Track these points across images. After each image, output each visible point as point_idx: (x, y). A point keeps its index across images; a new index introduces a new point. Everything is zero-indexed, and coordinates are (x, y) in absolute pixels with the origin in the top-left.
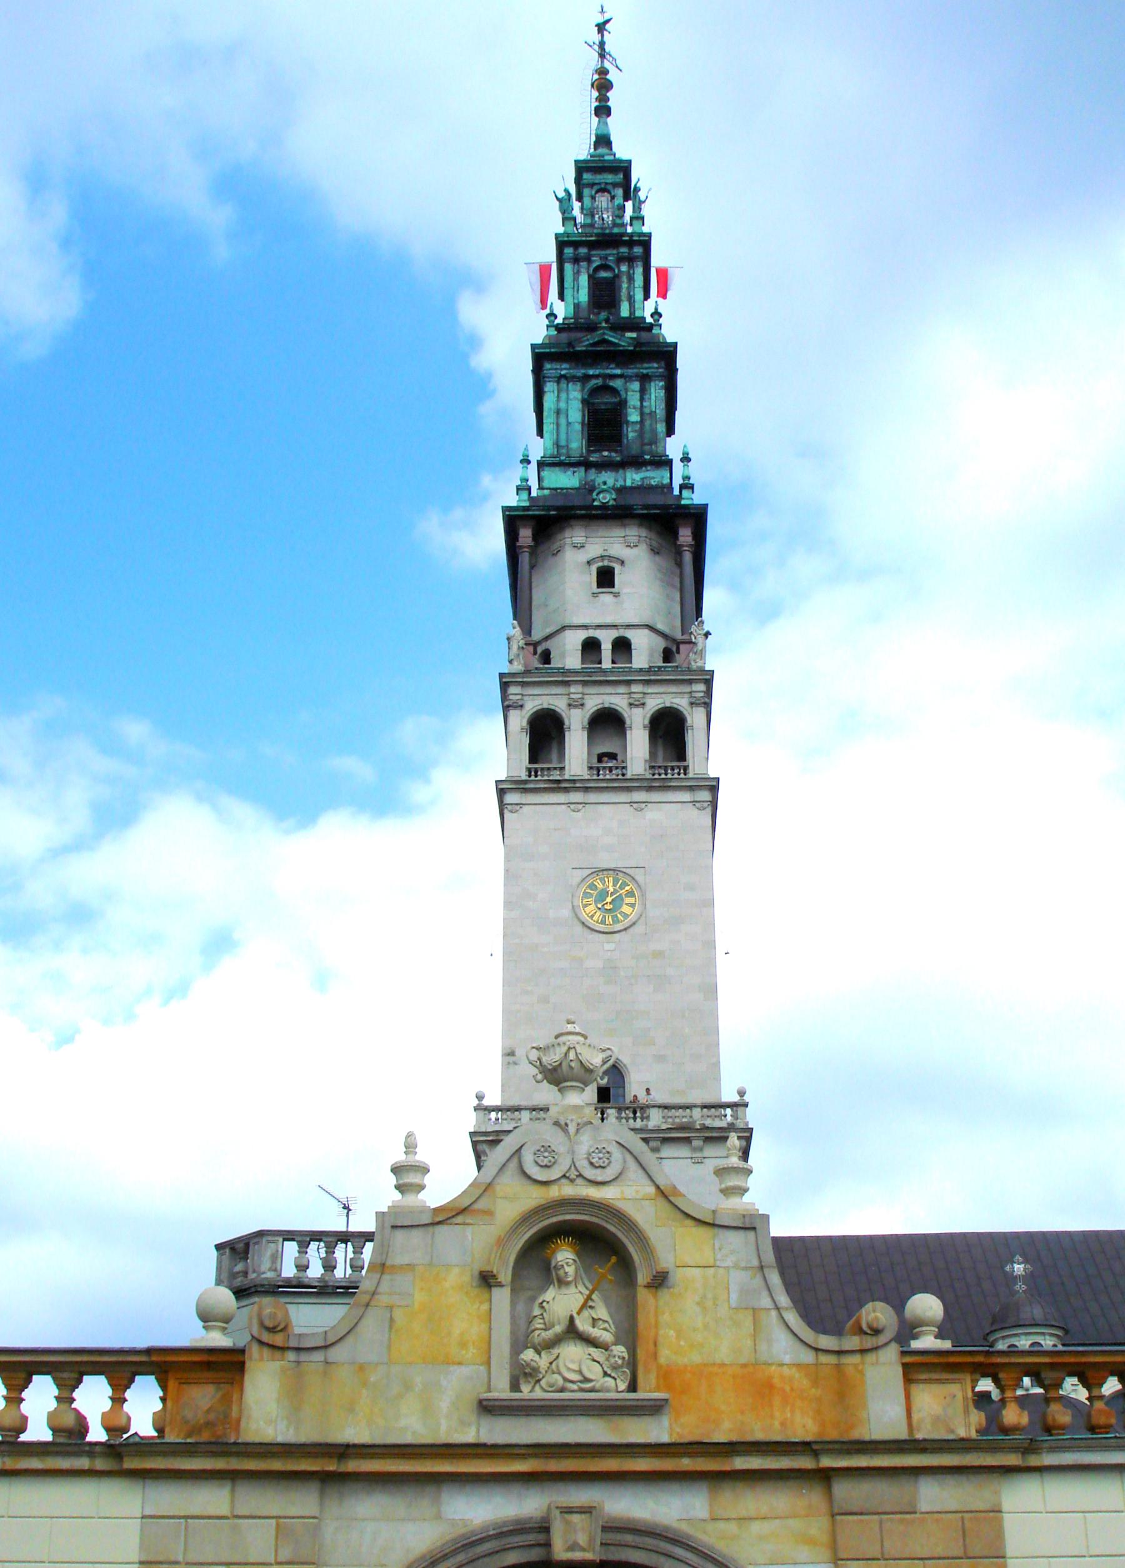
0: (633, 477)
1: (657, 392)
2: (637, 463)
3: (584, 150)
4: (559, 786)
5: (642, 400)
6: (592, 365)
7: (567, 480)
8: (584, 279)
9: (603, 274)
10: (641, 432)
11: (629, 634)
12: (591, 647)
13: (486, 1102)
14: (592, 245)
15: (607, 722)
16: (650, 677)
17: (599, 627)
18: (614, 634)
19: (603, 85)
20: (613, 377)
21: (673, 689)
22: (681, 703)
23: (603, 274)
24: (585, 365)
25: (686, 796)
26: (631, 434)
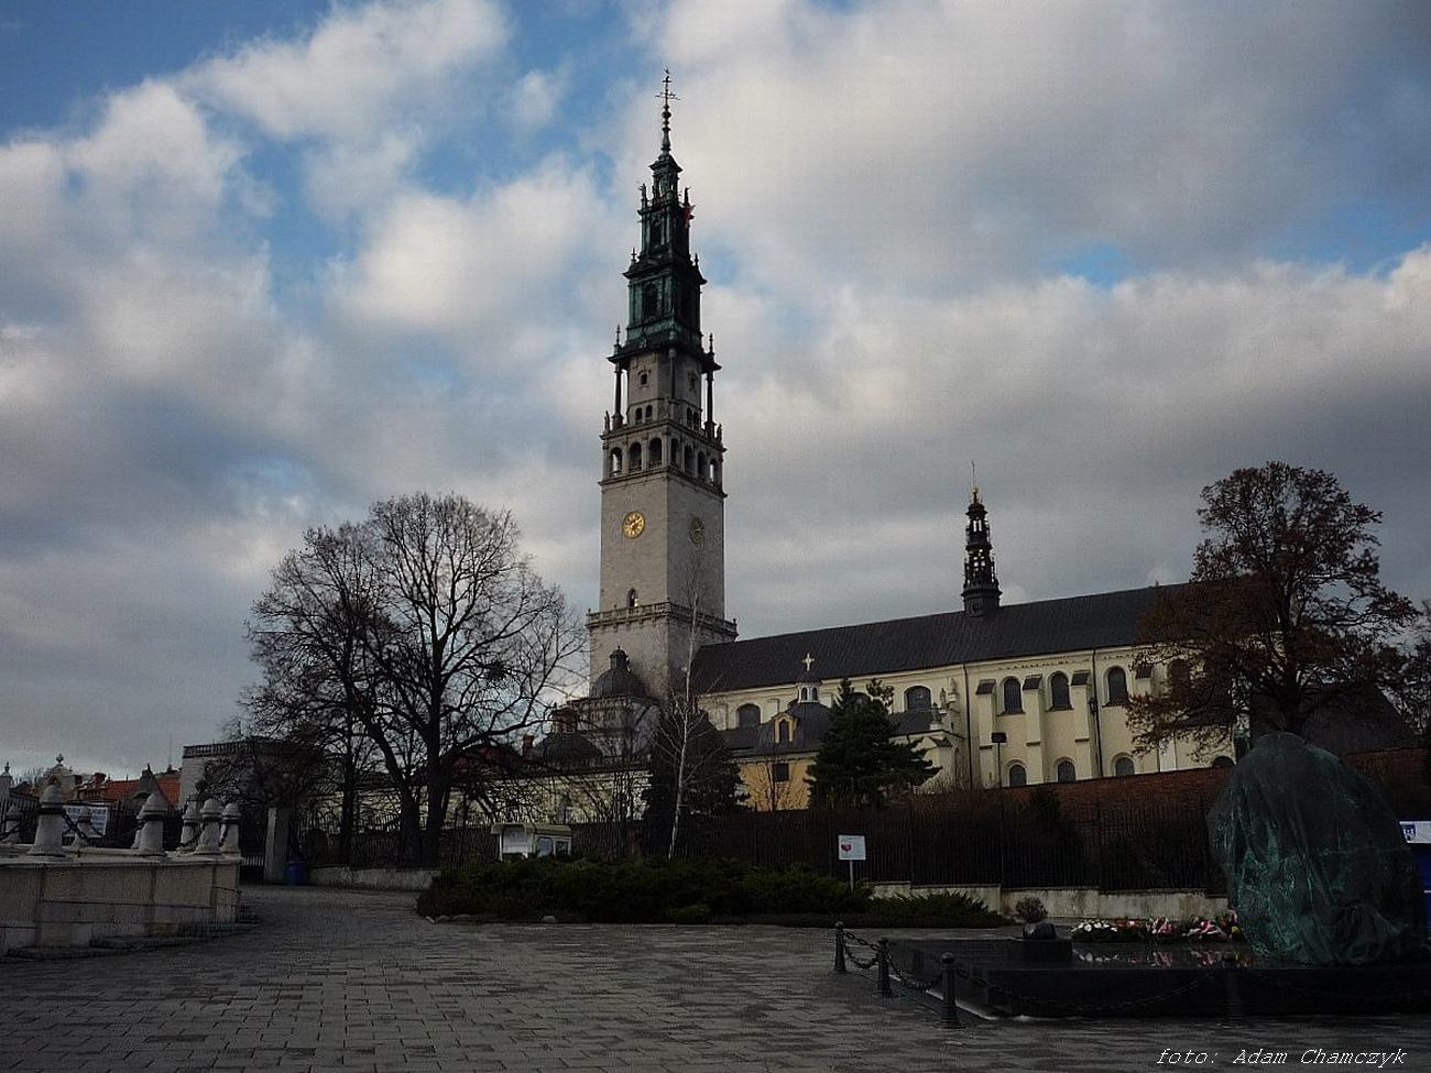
0: (658, 327)
1: (668, 283)
2: (659, 321)
3: (654, 159)
4: (618, 480)
7: (636, 334)
8: (648, 229)
11: (652, 404)
13: (592, 612)
14: (651, 212)
15: (636, 449)
16: (649, 426)
17: (641, 403)
18: (647, 404)
19: (667, 115)
20: (653, 280)
22: (660, 435)
23: (657, 224)
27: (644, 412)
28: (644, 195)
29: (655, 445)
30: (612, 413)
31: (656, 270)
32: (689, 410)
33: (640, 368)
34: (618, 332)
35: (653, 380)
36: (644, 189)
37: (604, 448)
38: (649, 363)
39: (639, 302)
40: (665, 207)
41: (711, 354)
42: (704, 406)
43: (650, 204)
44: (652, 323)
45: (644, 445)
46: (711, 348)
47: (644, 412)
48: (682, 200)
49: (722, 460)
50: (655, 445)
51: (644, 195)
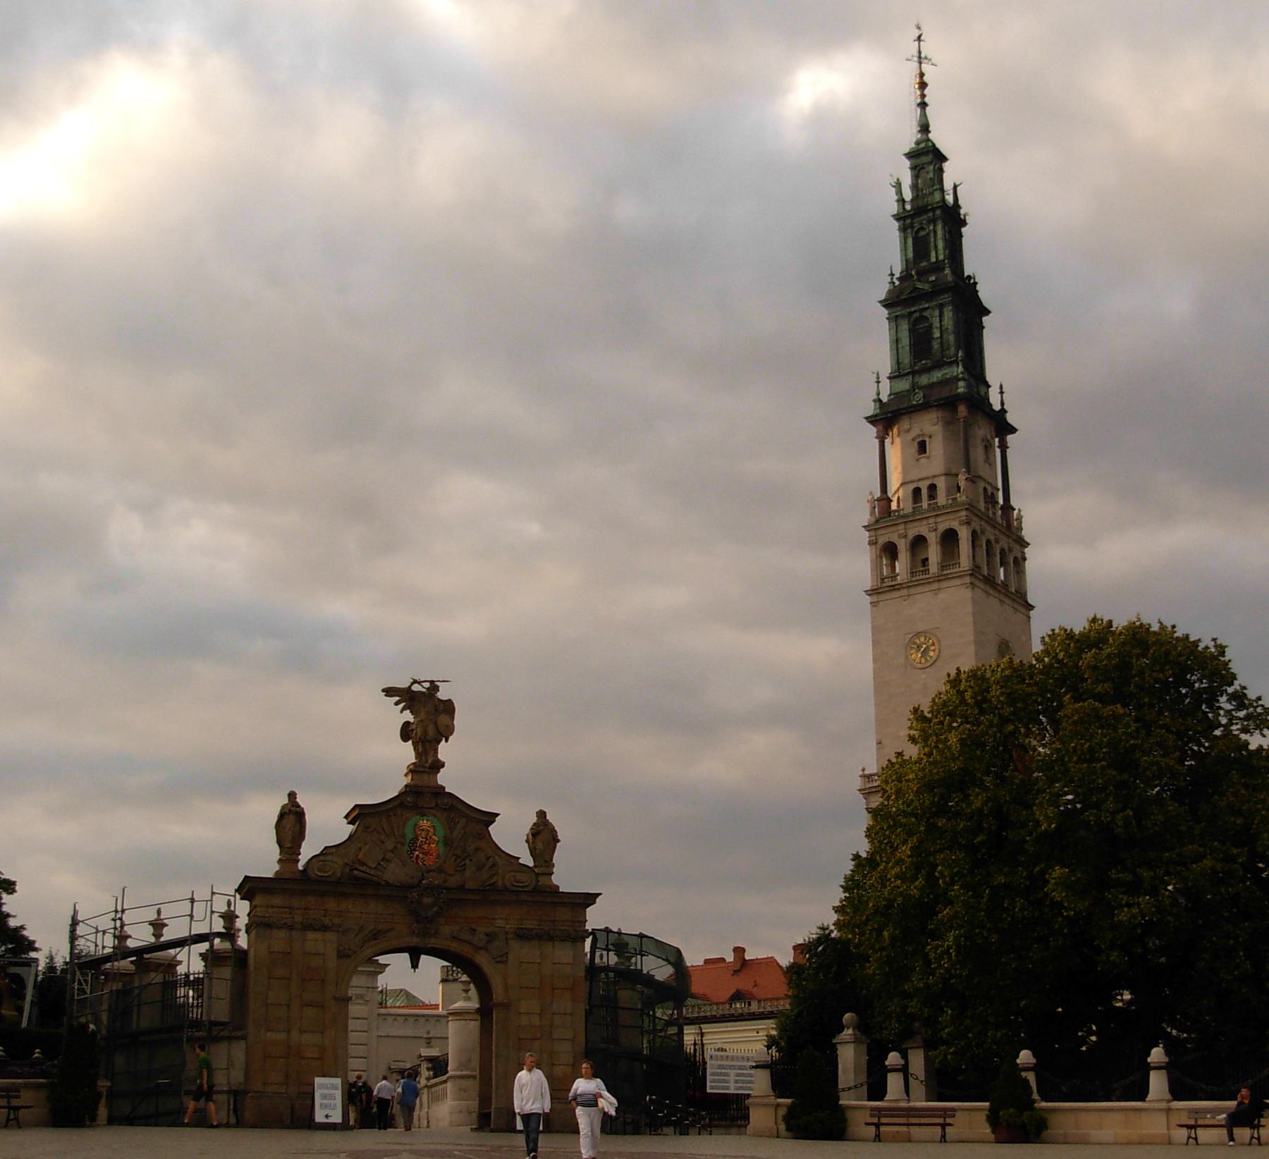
0: (937, 375)
1: (948, 314)
2: (939, 365)
4: (893, 588)
5: (941, 321)
6: (913, 305)
7: (904, 385)
9: (922, 233)
10: (942, 343)
12: (917, 492)
14: (912, 217)
15: (919, 542)
18: (928, 482)
19: (923, 85)
21: (951, 516)
22: (955, 525)
23: (922, 233)
24: (909, 306)
25: (957, 582)
26: (936, 345)
27: (924, 492)
28: (899, 192)
29: (950, 538)
30: (878, 494)
31: (929, 296)
32: (985, 489)
33: (915, 431)
34: (878, 382)
35: (937, 447)
36: (898, 185)
37: (870, 543)
38: (929, 424)
39: (905, 341)
40: (933, 210)
41: (1003, 411)
42: (1000, 485)
43: (908, 207)
44: (927, 370)
45: (933, 539)
46: (1002, 404)
47: (924, 492)
48: (950, 199)
49: (1025, 559)
50: (950, 538)
51: (899, 192)
